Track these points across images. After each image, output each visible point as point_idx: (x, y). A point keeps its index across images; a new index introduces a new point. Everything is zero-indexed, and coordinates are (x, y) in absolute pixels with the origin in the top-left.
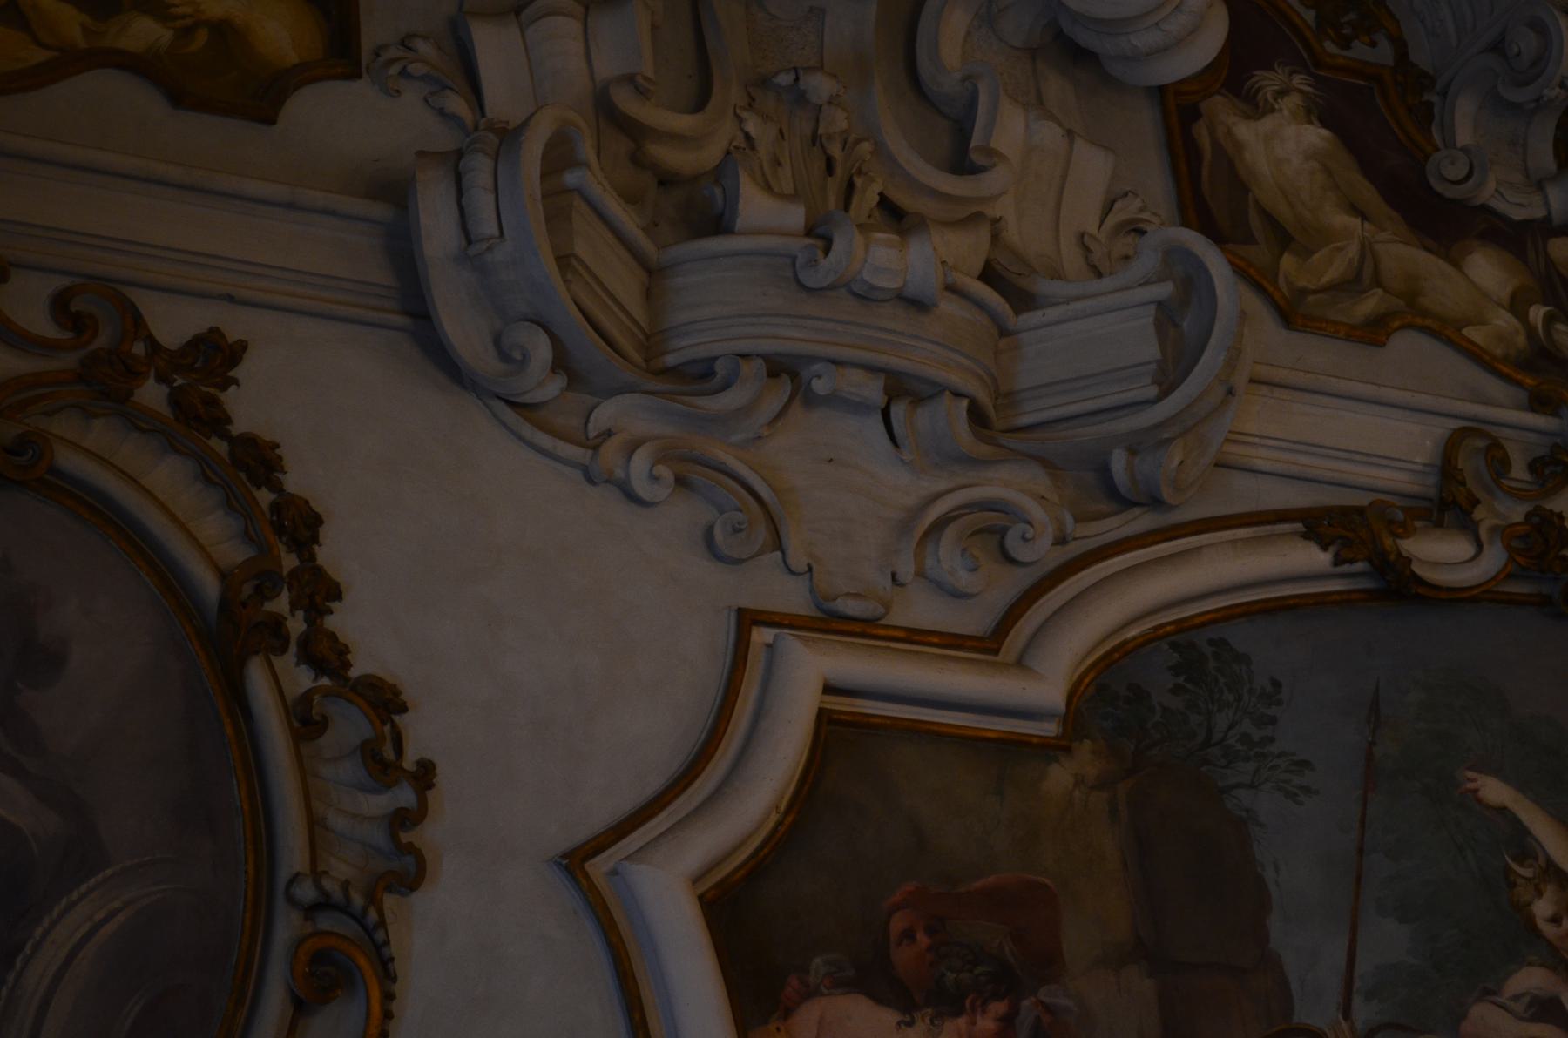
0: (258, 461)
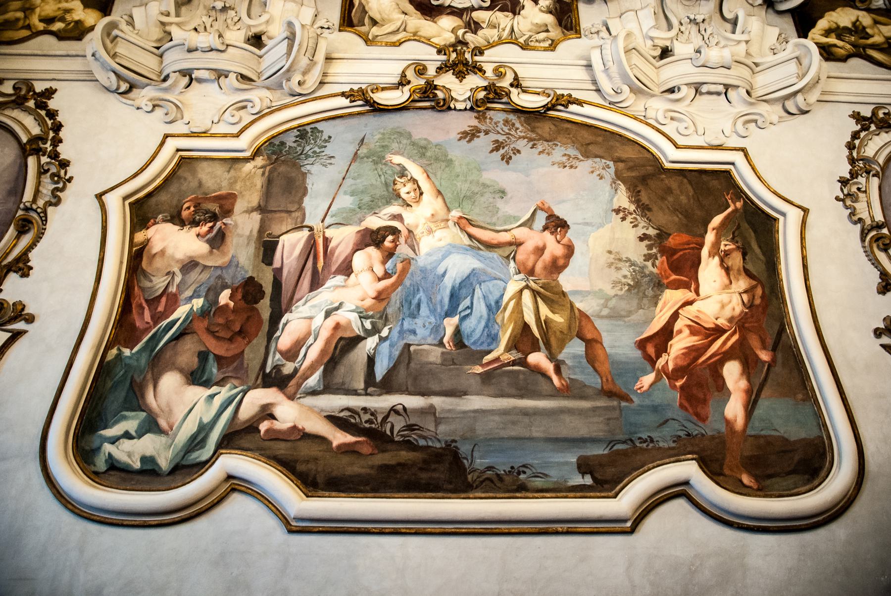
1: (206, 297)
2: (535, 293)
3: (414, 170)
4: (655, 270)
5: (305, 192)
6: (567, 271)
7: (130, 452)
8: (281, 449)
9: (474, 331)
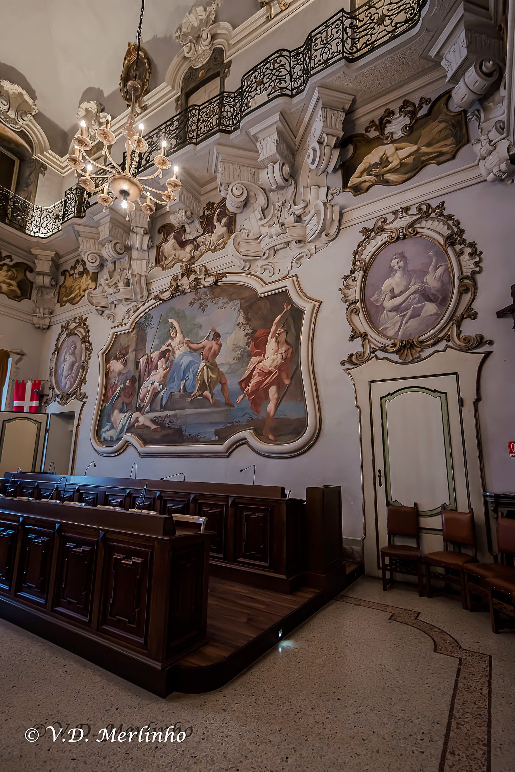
2: (208, 367)
3: (176, 324)
4: (249, 349)
8: (139, 431)
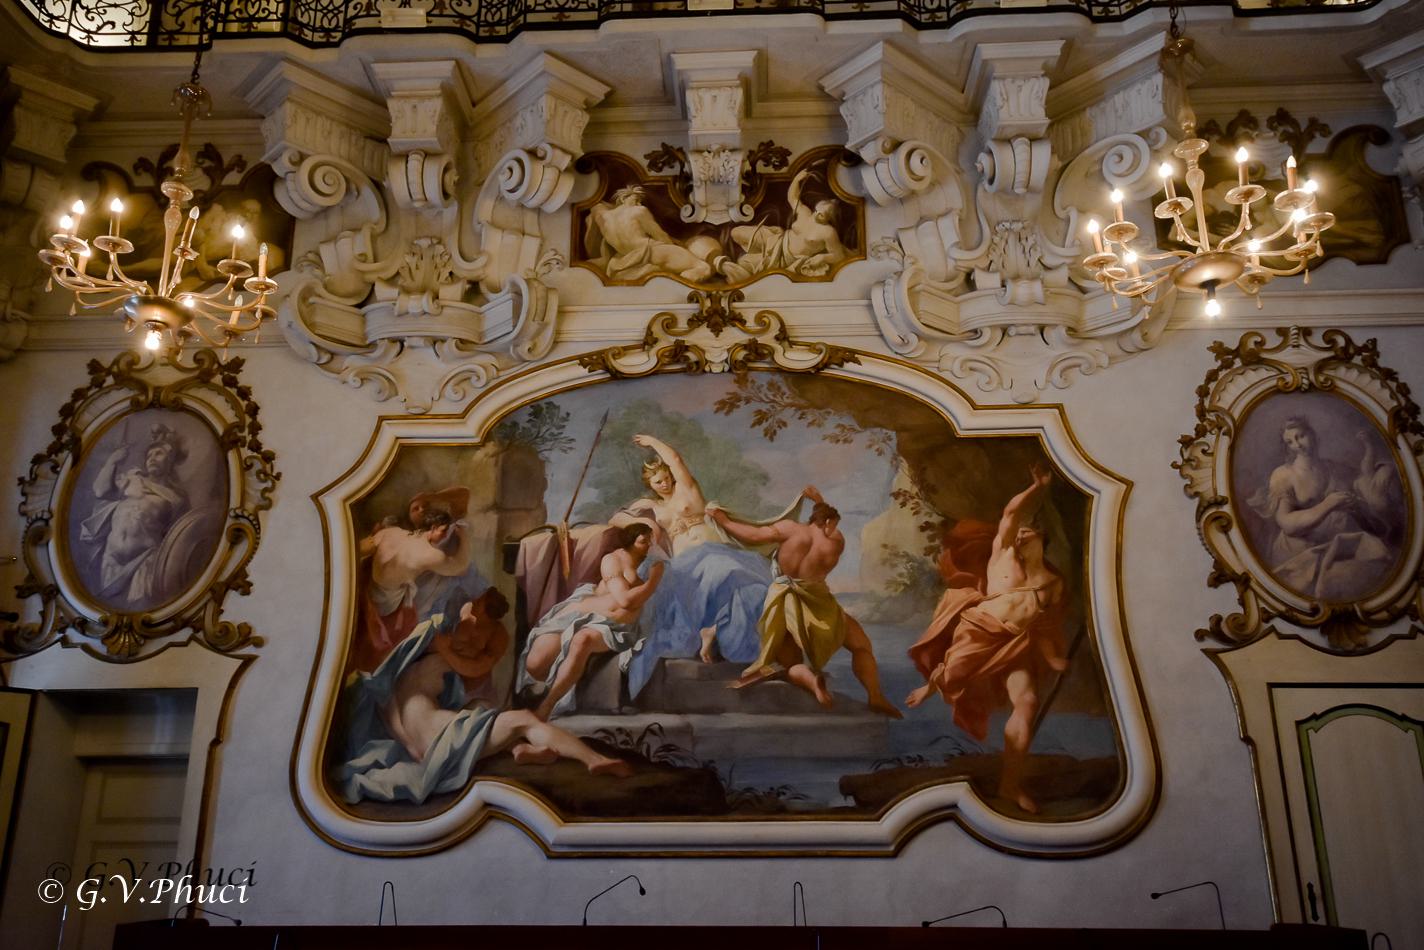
0: (245, 393)
1: (446, 612)
2: (799, 598)
3: (666, 454)
4: (936, 566)
5: (544, 485)
6: (835, 571)
7: (383, 781)
8: (537, 773)
9: (733, 641)
